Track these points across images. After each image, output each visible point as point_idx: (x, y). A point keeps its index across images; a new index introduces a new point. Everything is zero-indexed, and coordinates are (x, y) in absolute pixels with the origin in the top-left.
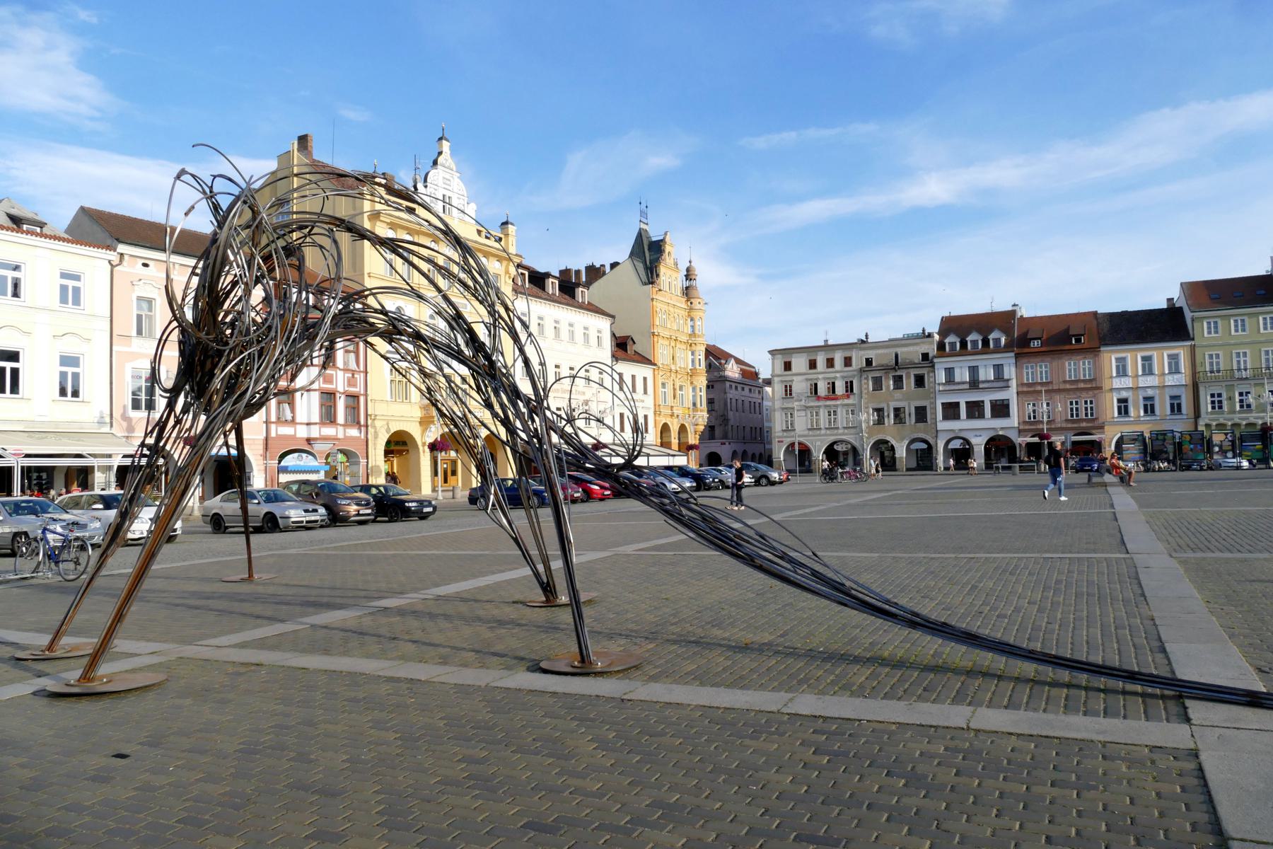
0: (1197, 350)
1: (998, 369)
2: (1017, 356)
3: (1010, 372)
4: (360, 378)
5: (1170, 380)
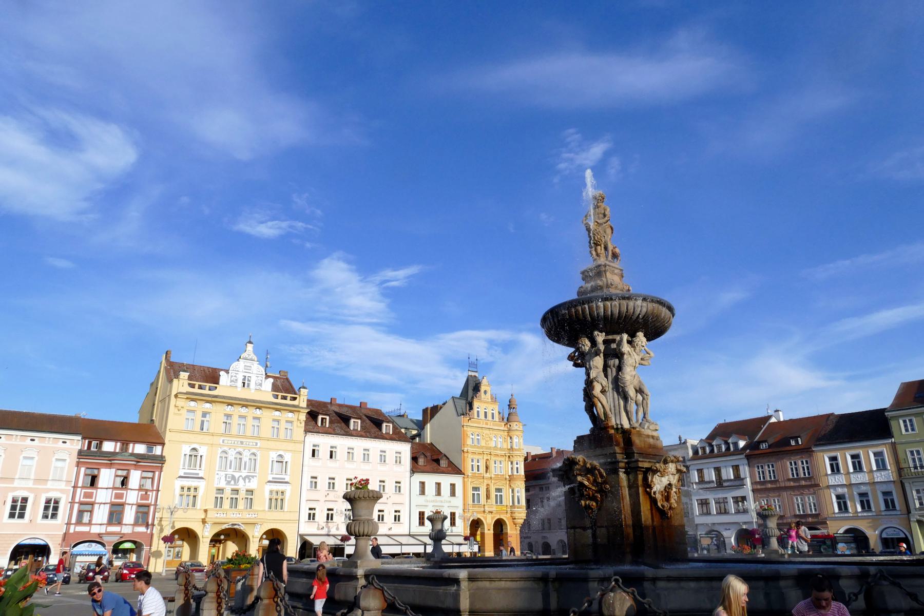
0: (900, 448)
1: (736, 468)
2: (748, 457)
3: (745, 471)
4: (152, 495)
5: (880, 477)
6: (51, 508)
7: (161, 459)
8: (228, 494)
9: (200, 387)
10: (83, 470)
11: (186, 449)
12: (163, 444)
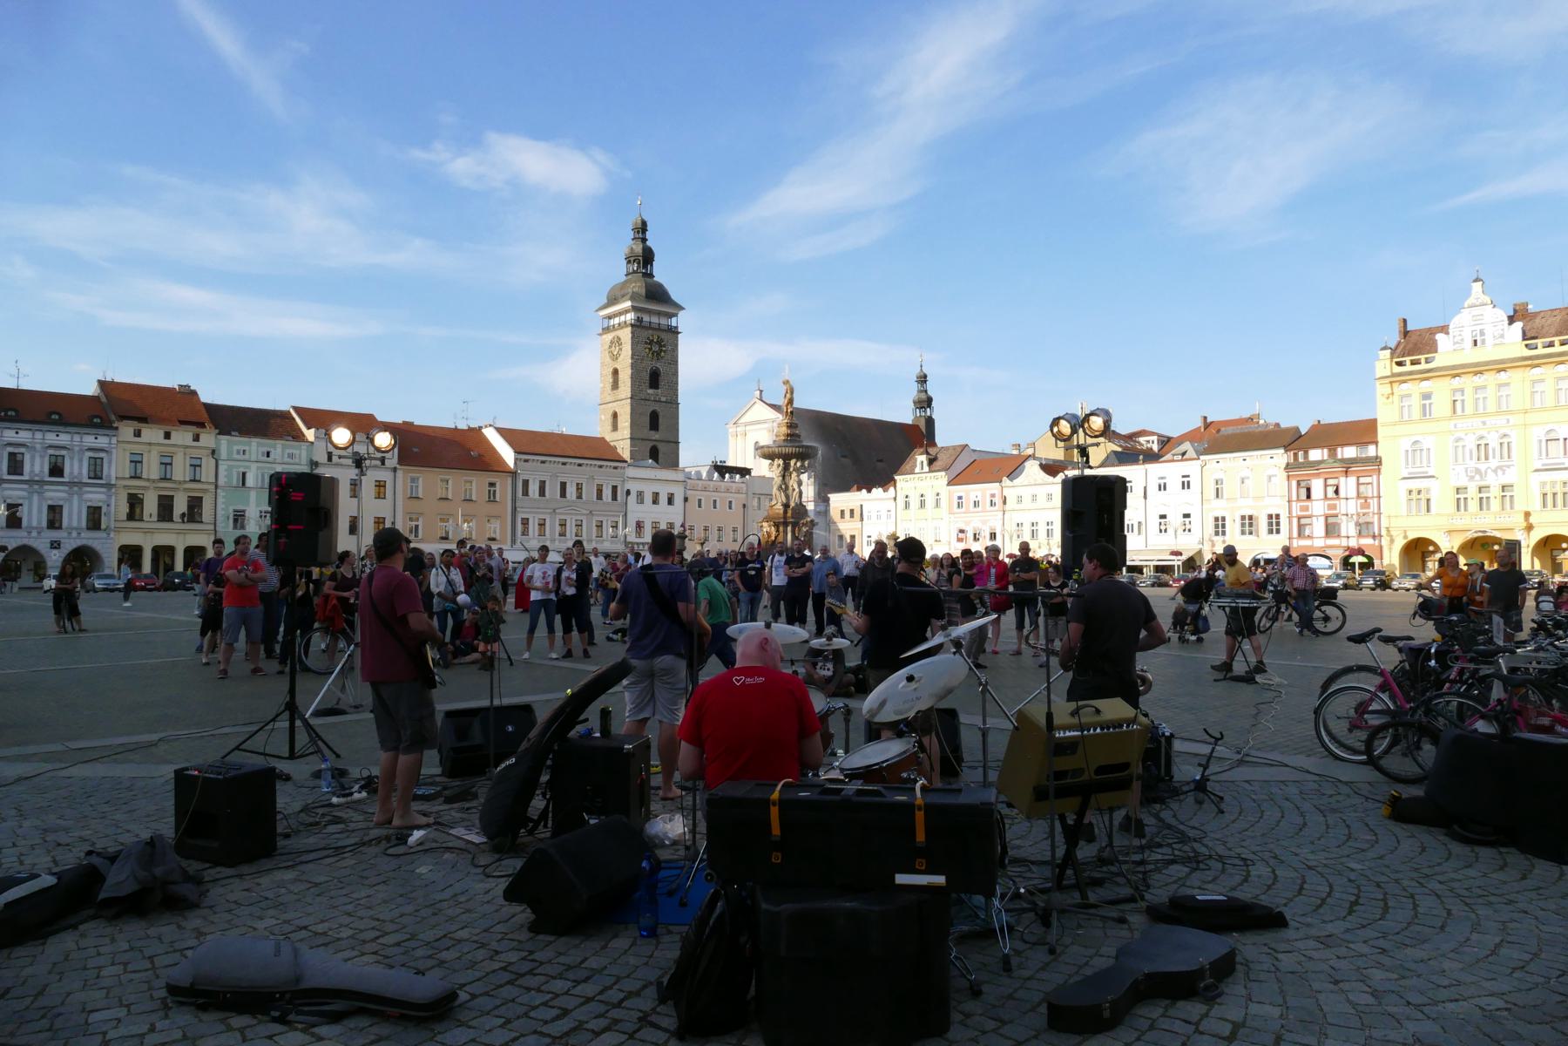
4: (1373, 503)
6: (1274, 524)
7: (1377, 461)
8: (1472, 493)
9: (1413, 363)
10: (1294, 483)
11: (1406, 444)
12: (1376, 443)
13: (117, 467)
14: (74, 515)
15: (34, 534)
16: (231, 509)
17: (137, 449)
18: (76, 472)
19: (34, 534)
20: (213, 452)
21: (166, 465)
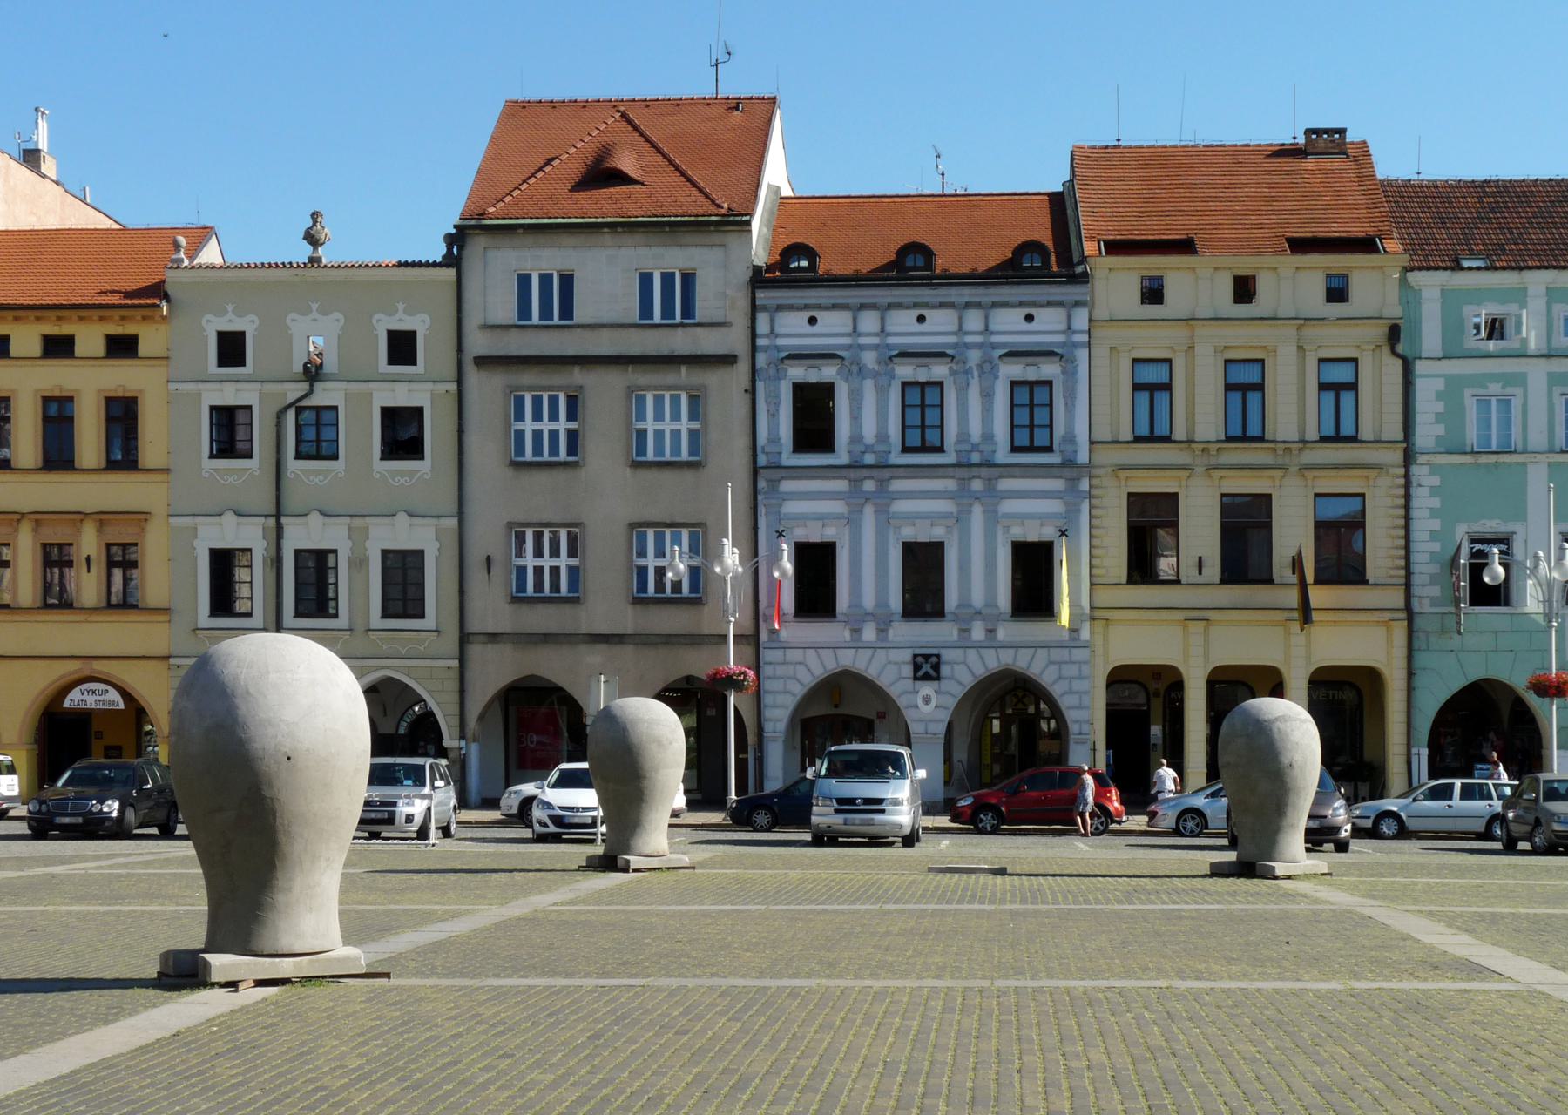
13: (1092, 409)
14: (979, 576)
15: (869, 633)
16: (1461, 532)
17: (1152, 342)
18: (975, 430)
19: (869, 633)
20: (1394, 334)
21: (1245, 386)
